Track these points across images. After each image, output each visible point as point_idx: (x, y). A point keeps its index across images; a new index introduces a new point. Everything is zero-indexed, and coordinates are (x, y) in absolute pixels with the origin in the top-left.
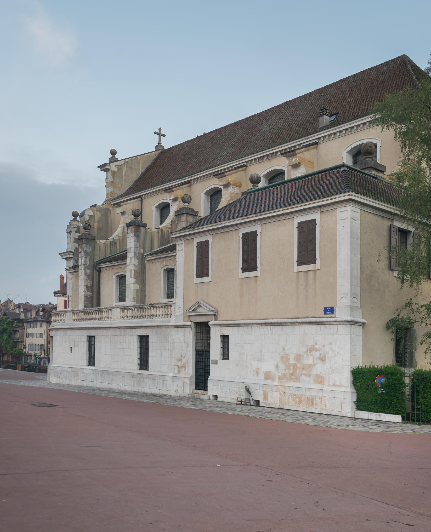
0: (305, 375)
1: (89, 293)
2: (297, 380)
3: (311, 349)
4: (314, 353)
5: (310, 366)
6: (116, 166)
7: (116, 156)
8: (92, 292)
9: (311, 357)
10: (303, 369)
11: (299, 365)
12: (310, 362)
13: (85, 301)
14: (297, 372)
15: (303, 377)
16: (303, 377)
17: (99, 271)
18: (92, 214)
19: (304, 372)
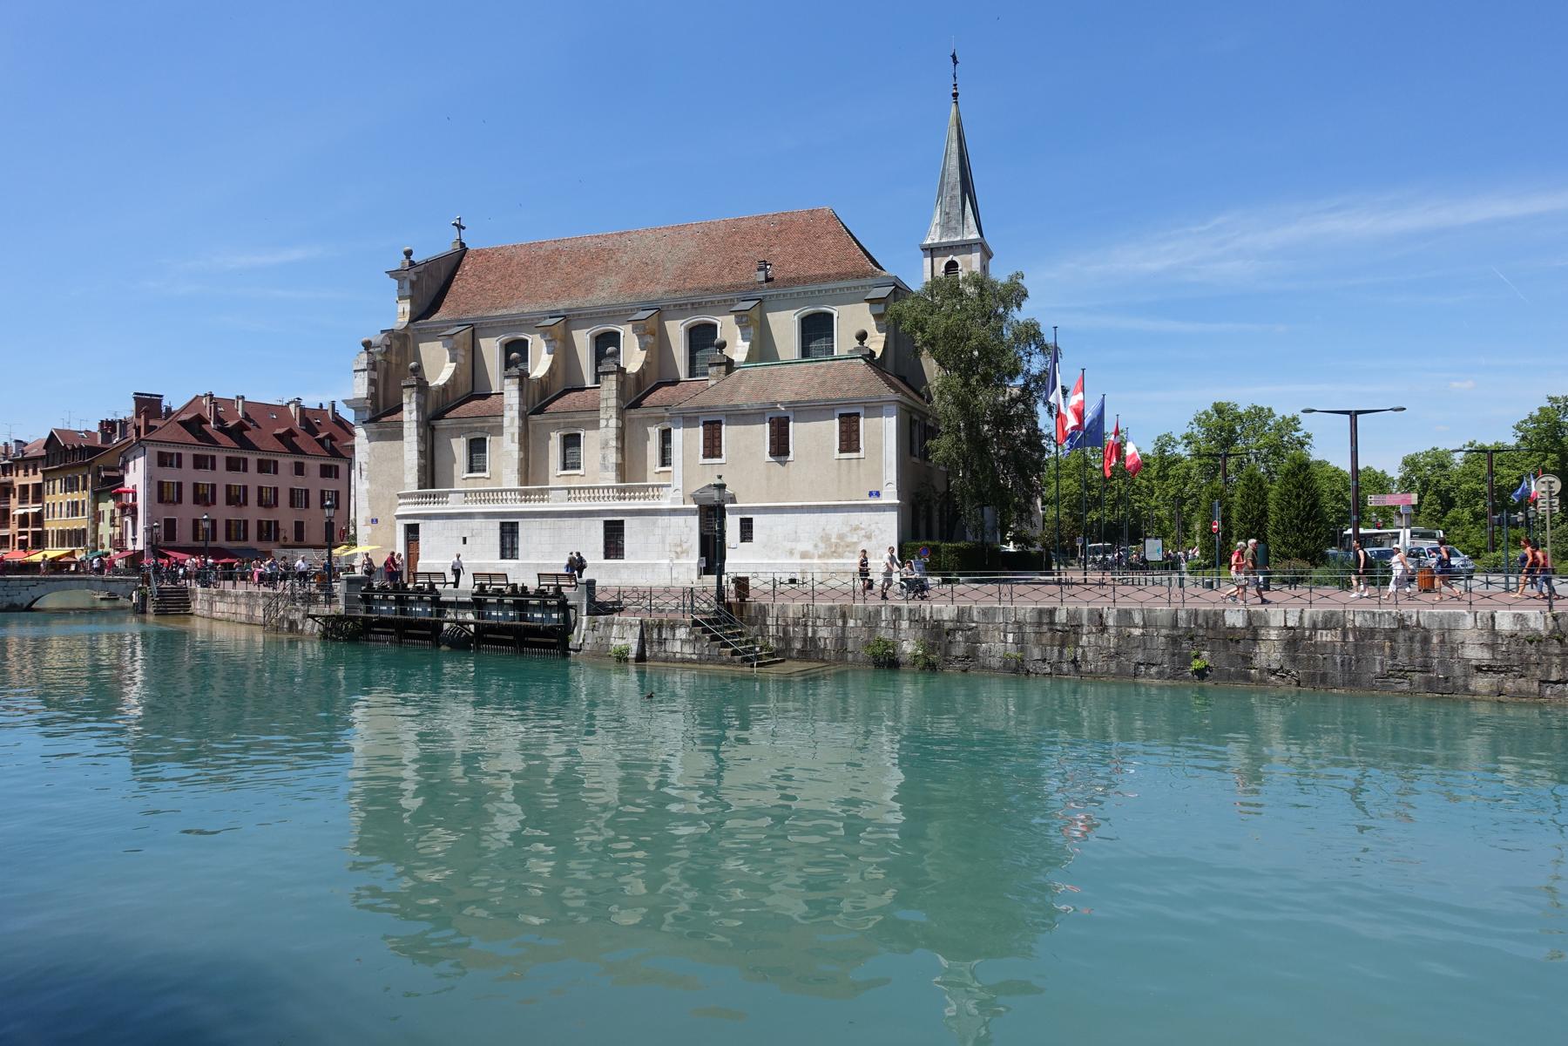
0: (849, 552)
1: (423, 461)
2: (841, 556)
3: (856, 529)
4: (859, 532)
5: (855, 543)
6: (416, 273)
7: (412, 258)
8: (426, 460)
9: (855, 536)
10: (847, 546)
11: (842, 544)
12: (855, 540)
13: (419, 471)
14: (840, 550)
15: (847, 553)
16: (847, 553)
17: (433, 429)
18: (389, 343)
19: (848, 549)
